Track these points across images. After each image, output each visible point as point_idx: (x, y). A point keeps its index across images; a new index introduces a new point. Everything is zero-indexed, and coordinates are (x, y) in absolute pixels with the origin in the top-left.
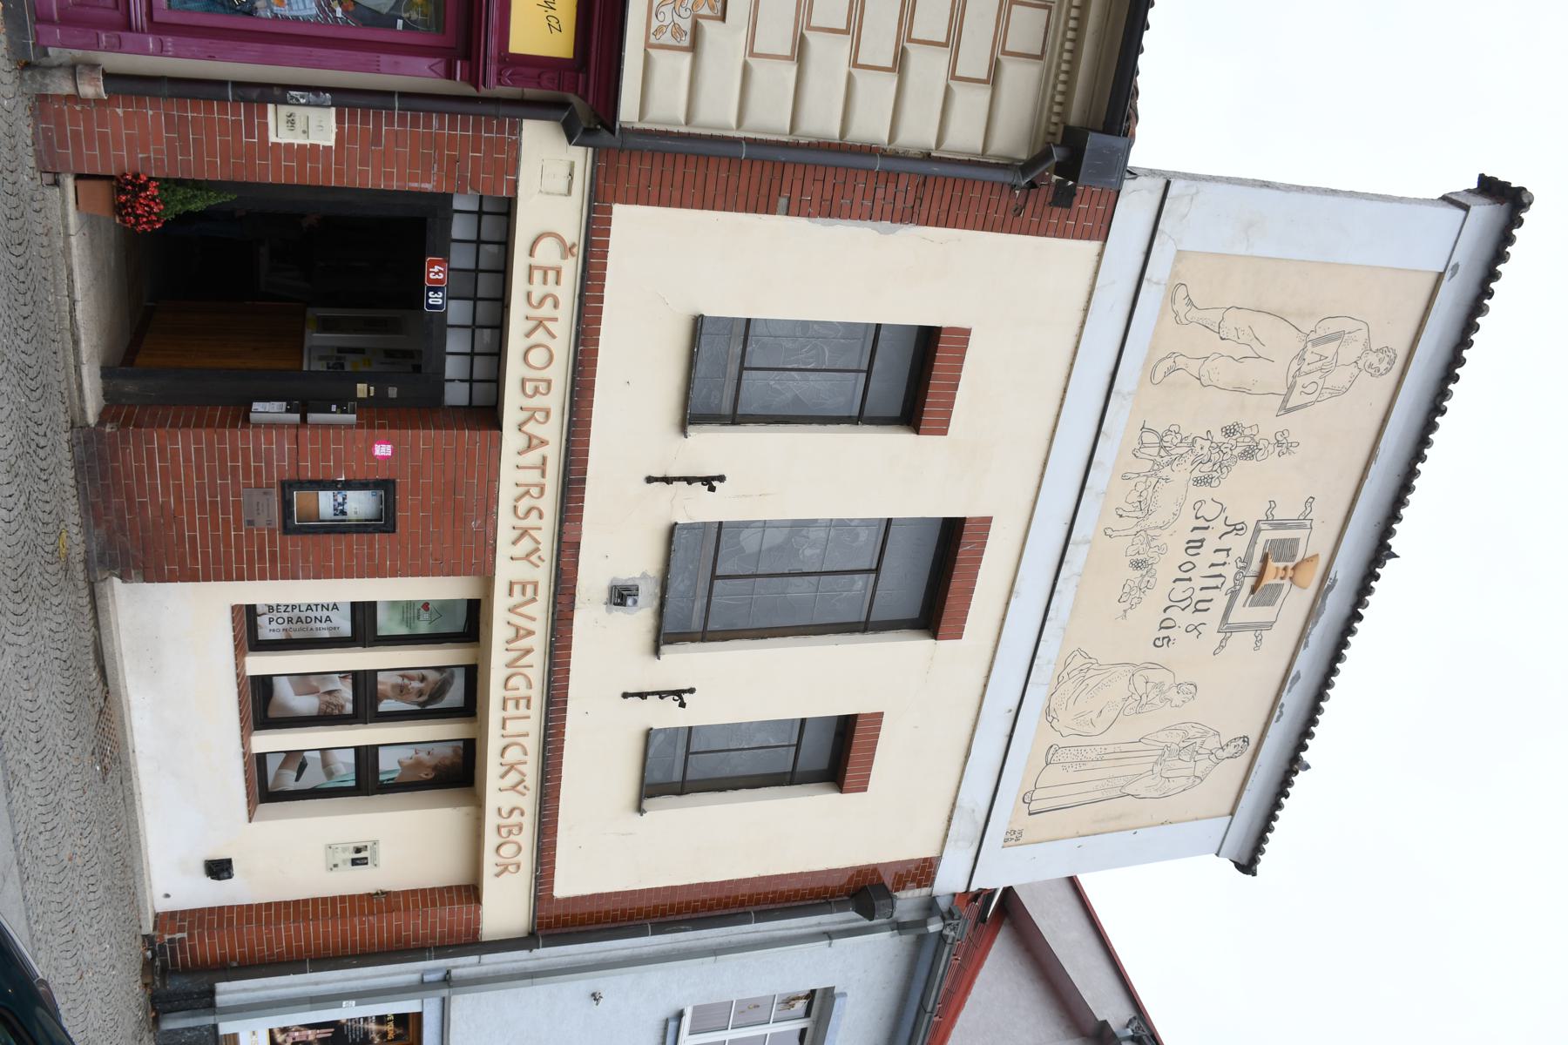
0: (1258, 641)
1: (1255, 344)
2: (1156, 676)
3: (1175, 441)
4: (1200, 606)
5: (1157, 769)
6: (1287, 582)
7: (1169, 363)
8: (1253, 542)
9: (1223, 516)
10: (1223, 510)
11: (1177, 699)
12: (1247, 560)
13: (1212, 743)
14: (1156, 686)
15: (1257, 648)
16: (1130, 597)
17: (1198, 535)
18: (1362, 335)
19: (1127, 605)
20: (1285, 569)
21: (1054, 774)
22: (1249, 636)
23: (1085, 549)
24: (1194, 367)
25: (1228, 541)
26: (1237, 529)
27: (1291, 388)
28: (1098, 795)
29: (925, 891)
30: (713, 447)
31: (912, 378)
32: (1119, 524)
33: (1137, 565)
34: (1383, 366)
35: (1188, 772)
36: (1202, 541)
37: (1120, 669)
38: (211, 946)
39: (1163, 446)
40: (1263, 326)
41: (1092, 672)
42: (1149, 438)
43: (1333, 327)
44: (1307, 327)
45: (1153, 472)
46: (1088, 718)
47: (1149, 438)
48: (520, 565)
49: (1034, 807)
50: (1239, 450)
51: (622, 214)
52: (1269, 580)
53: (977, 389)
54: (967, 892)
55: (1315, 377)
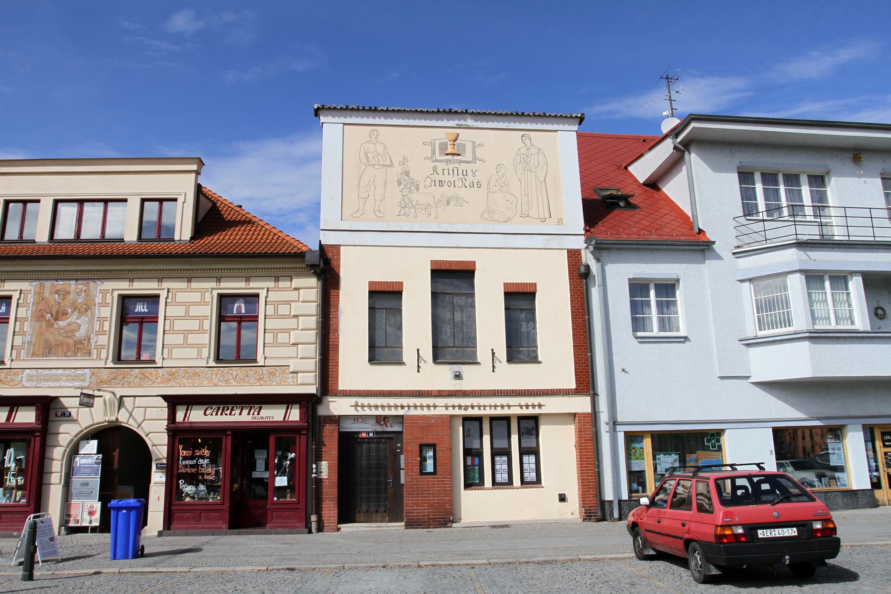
2: (493, 183)
5: (534, 170)
8: (440, 161)
11: (503, 171)
12: (447, 161)
13: (523, 151)
15: (483, 145)
16: (460, 201)
24: (378, 203)
25: (439, 171)
26: (435, 169)
27: (384, 165)
28: (544, 192)
29: (583, 252)
30: (408, 354)
31: (385, 298)
32: (433, 215)
33: (448, 203)
35: (536, 156)
38: (593, 501)
39: (405, 207)
42: (402, 213)
43: (363, 157)
44: (363, 166)
45: (414, 207)
47: (402, 213)
48: (441, 408)
49: (547, 216)
51: (340, 388)
53: (385, 276)
55: (380, 157)
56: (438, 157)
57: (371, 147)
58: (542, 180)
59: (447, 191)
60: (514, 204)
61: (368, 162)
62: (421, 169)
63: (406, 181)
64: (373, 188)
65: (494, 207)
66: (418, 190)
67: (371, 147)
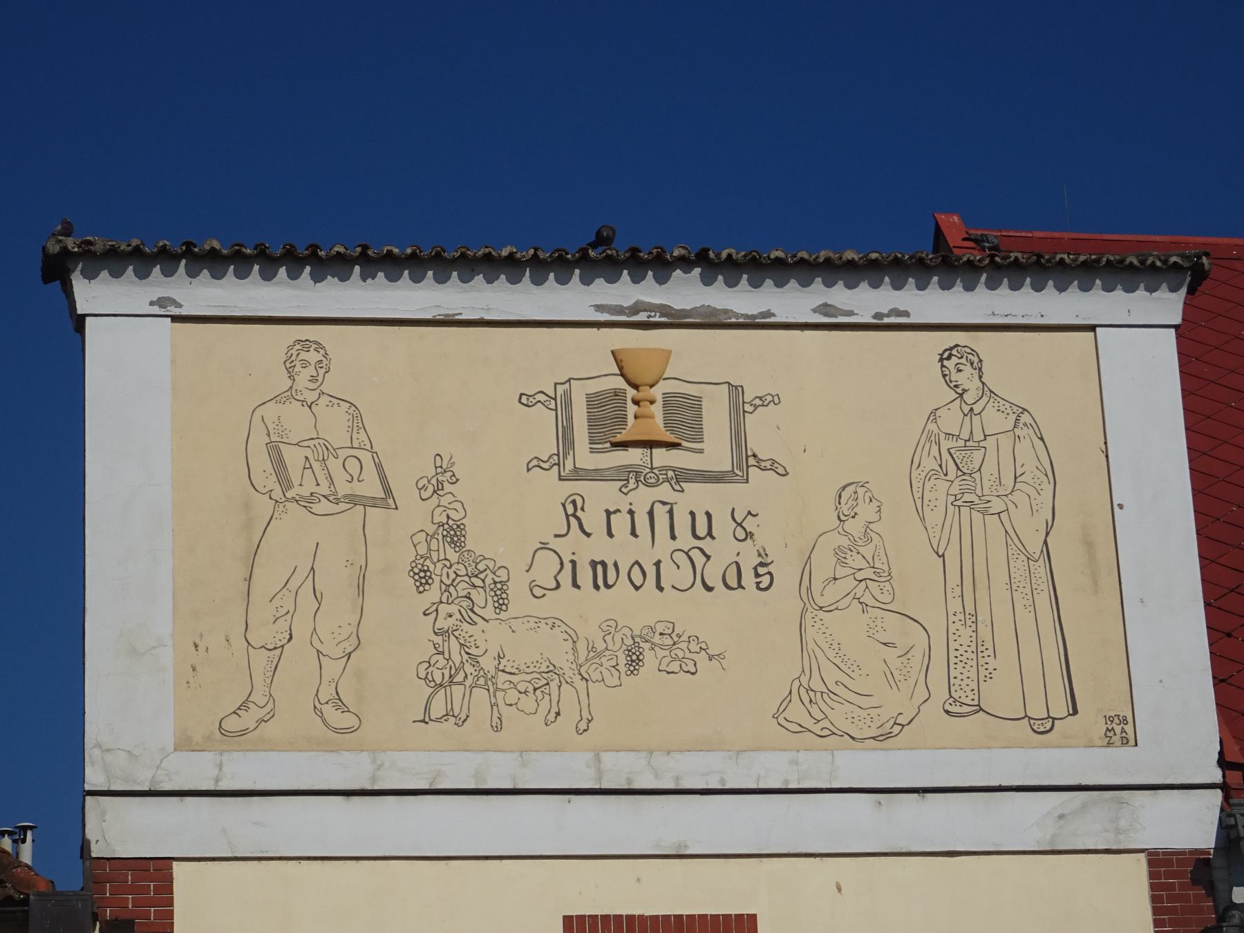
0: (763, 401)
1: (293, 585)
2: (824, 564)
3: (442, 662)
4: (702, 531)
6: (657, 392)
7: (328, 710)
9: (555, 544)
10: (544, 546)
11: (866, 512)
12: (627, 476)
13: (951, 420)
14: (842, 562)
15: (776, 400)
17: (585, 576)
18: (271, 411)
19: (702, 658)
20: (636, 402)
21: (1001, 694)
22: (752, 422)
23: (608, 759)
24: (332, 669)
25: (593, 518)
26: (573, 511)
27: (354, 500)
28: (1043, 601)
33: (635, 661)
34: (313, 357)
35: (1006, 442)
36: (594, 564)
37: (810, 633)
40: (266, 581)
41: (817, 684)
42: (438, 709)
44: (263, 506)
45: (489, 683)
46: (895, 663)
47: (438, 709)
49: (1059, 707)
50: (453, 556)
52: (657, 426)
54: (1224, 787)
56: (584, 457)
57: (296, 422)
58: (1035, 547)
59: (633, 608)
60: (917, 658)
61: (285, 484)
62: (514, 514)
63: (452, 568)
64: (307, 601)
65: (831, 675)
66: (501, 605)
67: (296, 422)
